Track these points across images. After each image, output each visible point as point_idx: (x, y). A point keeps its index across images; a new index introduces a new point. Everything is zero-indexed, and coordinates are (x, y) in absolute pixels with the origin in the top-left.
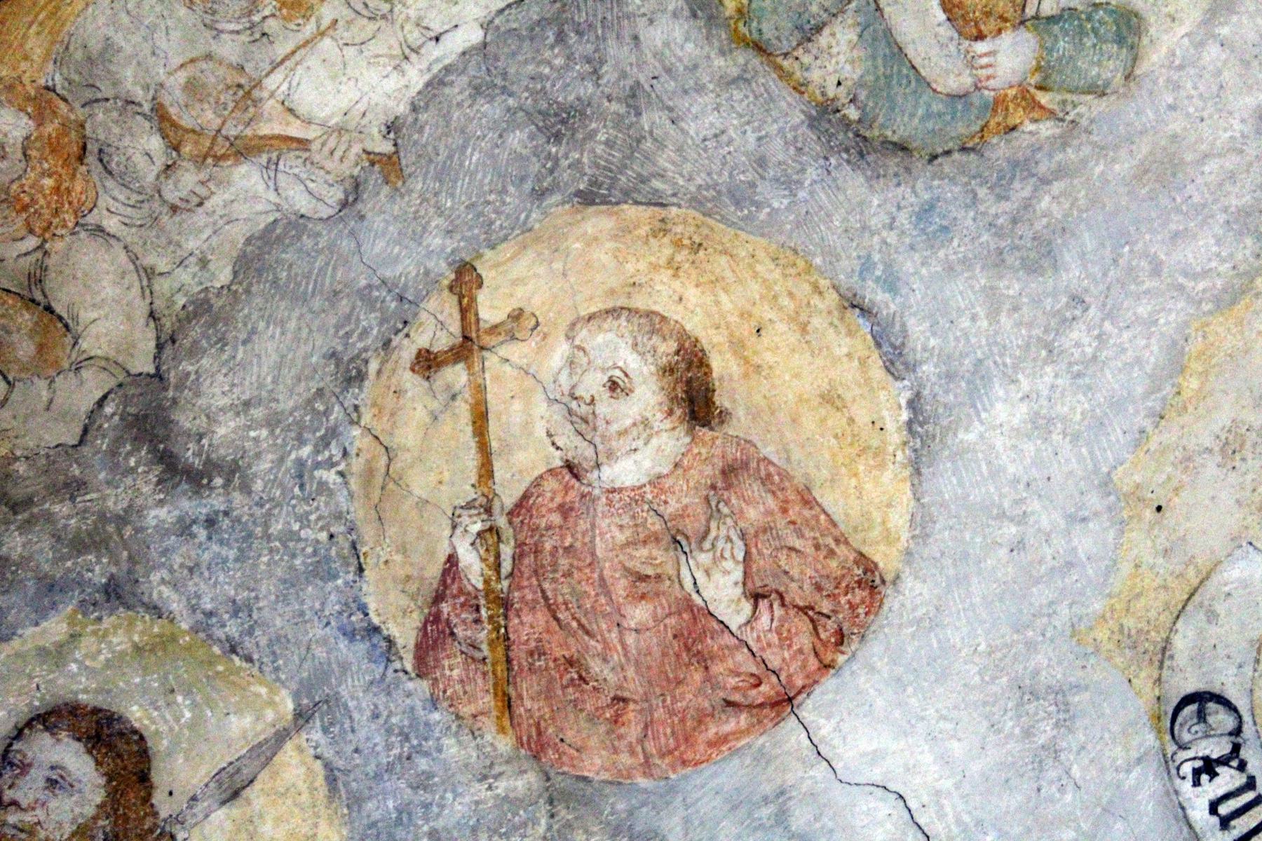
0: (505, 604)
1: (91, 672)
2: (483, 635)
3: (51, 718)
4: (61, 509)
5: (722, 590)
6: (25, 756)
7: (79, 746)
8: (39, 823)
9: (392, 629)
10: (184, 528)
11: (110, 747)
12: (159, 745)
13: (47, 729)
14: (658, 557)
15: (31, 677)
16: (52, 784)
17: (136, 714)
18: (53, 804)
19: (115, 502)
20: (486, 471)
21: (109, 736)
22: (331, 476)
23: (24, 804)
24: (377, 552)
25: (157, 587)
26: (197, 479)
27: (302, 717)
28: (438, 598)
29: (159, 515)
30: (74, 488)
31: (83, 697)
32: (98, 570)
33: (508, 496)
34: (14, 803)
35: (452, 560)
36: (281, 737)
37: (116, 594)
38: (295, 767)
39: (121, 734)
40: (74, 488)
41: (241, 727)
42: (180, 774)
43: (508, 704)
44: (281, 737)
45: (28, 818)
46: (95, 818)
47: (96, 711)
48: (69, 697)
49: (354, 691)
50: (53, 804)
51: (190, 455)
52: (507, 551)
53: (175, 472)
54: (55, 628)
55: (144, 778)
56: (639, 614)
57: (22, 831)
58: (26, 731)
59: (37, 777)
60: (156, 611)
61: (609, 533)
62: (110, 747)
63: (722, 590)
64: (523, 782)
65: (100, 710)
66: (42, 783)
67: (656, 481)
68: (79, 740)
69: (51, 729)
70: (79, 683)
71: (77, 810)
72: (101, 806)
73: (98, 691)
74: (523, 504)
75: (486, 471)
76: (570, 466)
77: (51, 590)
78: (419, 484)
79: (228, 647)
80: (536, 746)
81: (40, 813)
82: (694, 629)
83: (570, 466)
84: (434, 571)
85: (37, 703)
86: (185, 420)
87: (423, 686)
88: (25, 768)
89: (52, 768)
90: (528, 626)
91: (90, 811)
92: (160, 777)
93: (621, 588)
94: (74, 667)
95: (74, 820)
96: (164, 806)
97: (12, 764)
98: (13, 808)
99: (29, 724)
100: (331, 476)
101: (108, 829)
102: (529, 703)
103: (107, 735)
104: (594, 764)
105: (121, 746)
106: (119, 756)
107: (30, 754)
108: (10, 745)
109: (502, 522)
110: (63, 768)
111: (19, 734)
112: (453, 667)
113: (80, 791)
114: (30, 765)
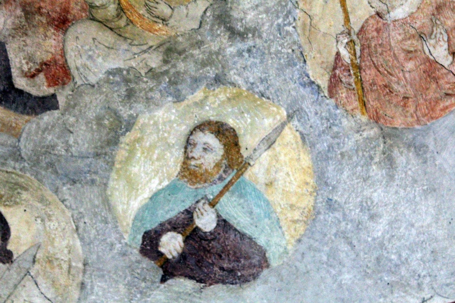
0: (359, 68)
1: (213, 109)
2: (352, 80)
3: (201, 127)
4: (196, 52)
5: (440, 53)
6: (194, 141)
7: (213, 136)
8: (202, 164)
9: (319, 82)
10: (240, 54)
11: (224, 134)
12: (241, 132)
13: (201, 130)
14: (415, 43)
15: (193, 113)
16: (205, 149)
17: (231, 122)
18: (206, 156)
19: (214, 47)
20: (347, 19)
21: (223, 131)
22: (290, 29)
23: (196, 157)
24: (310, 55)
25: (233, 75)
26: (242, 36)
27: (290, 117)
28: (335, 68)
29: (231, 50)
30: (199, 44)
31: (212, 118)
32: (211, 72)
33: (356, 28)
34: (193, 158)
35: (338, 54)
36: (283, 125)
37: (219, 80)
38: (289, 135)
39: (227, 130)
40: (199, 44)
41: (268, 123)
42: (248, 142)
43: (364, 104)
44: (283, 125)
45: (199, 162)
46: (221, 160)
47: (217, 122)
48: (207, 119)
49: (308, 106)
50: (206, 156)
51: (239, 27)
52: (358, 48)
53: (235, 34)
54: (199, 95)
55: (236, 144)
56: (410, 65)
57: (197, 167)
58: (194, 132)
59: (199, 148)
60: (233, 84)
61: (395, 36)
62: (224, 134)
63: (440, 53)
64: (373, 132)
65: (219, 122)
66: (201, 150)
67: (411, 15)
68: (212, 133)
69: (202, 130)
70: (210, 113)
71: (215, 158)
72: (223, 156)
73: (217, 115)
74: (362, 30)
75: (347, 19)
76: (378, 14)
77: (196, 81)
78: (323, 27)
79: (261, 95)
80: (376, 118)
81: (202, 160)
82: (431, 68)
83: (378, 14)
84: (332, 59)
85: (196, 122)
86: (235, 14)
87: (333, 101)
88: (195, 145)
89: (205, 144)
90: (369, 75)
91: (219, 158)
92: (242, 143)
93: (402, 56)
94: (207, 108)
95: (214, 162)
96: (245, 154)
97: (190, 144)
98: (193, 159)
99: (194, 130)
100: (290, 29)
101: (226, 163)
102: (372, 103)
103: (221, 130)
104: (399, 123)
105: (227, 134)
106: (227, 137)
107: (196, 140)
108: (189, 138)
109: (355, 37)
110: (208, 144)
111: (191, 133)
112: (343, 93)
113: (215, 151)
114: (196, 144)
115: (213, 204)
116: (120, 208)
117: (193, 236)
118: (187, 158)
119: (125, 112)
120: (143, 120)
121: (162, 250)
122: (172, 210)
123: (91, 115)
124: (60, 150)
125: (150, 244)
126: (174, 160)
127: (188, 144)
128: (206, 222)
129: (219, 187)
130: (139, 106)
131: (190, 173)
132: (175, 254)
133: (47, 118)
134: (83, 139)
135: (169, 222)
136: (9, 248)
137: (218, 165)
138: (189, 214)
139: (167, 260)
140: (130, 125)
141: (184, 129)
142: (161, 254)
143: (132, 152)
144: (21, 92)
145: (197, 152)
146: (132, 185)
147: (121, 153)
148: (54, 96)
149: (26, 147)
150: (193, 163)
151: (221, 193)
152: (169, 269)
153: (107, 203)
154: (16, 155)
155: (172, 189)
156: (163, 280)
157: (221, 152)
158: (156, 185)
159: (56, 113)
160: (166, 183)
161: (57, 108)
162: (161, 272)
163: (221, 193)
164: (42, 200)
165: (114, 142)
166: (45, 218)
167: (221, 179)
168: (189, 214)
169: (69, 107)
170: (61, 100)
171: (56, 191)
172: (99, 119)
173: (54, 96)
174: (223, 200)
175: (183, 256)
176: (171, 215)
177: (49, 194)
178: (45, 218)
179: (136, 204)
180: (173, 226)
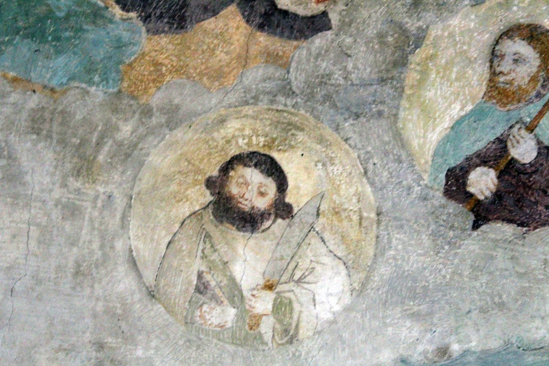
1: (524, 9)
3: (509, 33)
6: (501, 51)
7: (524, 43)
8: (513, 79)
11: (538, 40)
13: (509, 38)
15: (497, 17)
16: (516, 61)
18: (518, 70)
21: (537, 35)
23: (506, 72)
31: (522, 21)
34: (501, 73)
39: (542, 34)
45: (508, 78)
46: (538, 72)
47: (529, 26)
48: (516, 22)
50: (518, 70)
57: (507, 84)
58: (500, 41)
59: (508, 59)
62: (538, 40)
65: (531, 25)
66: (511, 62)
68: (524, 40)
69: (510, 37)
71: (529, 70)
72: (539, 66)
73: (528, 16)
81: (513, 75)
85: (502, 28)
88: (502, 56)
89: (515, 54)
91: (535, 70)
94: (515, 8)
95: (529, 75)
97: (497, 56)
98: (501, 75)
99: (500, 37)
101: (544, 76)
105: (543, 38)
106: (543, 43)
107: (504, 50)
108: (494, 48)
110: (519, 53)
111: (497, 43)
113: (528, 62)
114: (504, 55)
115: (530, 129)
116: (415, 143)
117: (508, 169)
118: (494, 74)
119: (412, 24)
120: (435, 32)
121: (471, 189)
122: (481, 140)
123: (371, 32)
124: (338, 77)
125: (456, 184)
126: (477, 77)
127: (494, 56)
128: (524, 151)
129: (538, 106)
130: (429, 16)
131: (499, 92)
132: (488, 193)
133: (319, 41)
134: (363, 62)
135: (478, 155)
136: (287, 200)
137: (533, 79)
138: (502, 143)
139: (478, 202)
140: (419, 40)
141: (487, 38)
142: (471, 195)
143: (424, 73)
144: (285, 13)
145: (505, 66)
146: (428, 114)
147: (412, 76)
148: (324, 14)
149: (297, 79)
150: (502, 79)
151: (541, 114)
152: (482, 213)
153: (399, 137)
154: (287, 90)
155: (478, 114)
156: (476, 226)
157: (537, 63)
158: (456, 111)
159: (329, 34)
160: (469, 107)
161: (330, 28)
162: (472, 217)
163: (541, 114)
164: (321, 140)
165: (401, 63)
166: (327, 162)
167: (539, 96)
168: (502, 143)
169: (345, 25)
170: (334, 18)
171: (337, 129)
172: (381, 36)
173: (324, 14)
174: (544, 121)
175: (498, 196)
176: (480, 146)
177: (328, 132)
178: (327, 162)
179: (434, 137)
180: (483, 159)
